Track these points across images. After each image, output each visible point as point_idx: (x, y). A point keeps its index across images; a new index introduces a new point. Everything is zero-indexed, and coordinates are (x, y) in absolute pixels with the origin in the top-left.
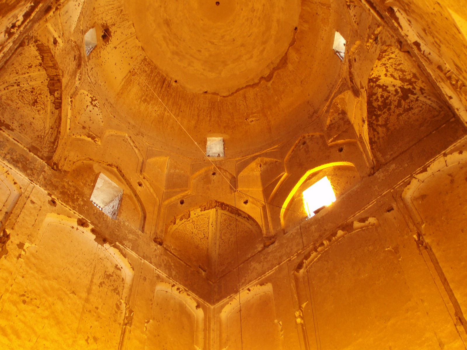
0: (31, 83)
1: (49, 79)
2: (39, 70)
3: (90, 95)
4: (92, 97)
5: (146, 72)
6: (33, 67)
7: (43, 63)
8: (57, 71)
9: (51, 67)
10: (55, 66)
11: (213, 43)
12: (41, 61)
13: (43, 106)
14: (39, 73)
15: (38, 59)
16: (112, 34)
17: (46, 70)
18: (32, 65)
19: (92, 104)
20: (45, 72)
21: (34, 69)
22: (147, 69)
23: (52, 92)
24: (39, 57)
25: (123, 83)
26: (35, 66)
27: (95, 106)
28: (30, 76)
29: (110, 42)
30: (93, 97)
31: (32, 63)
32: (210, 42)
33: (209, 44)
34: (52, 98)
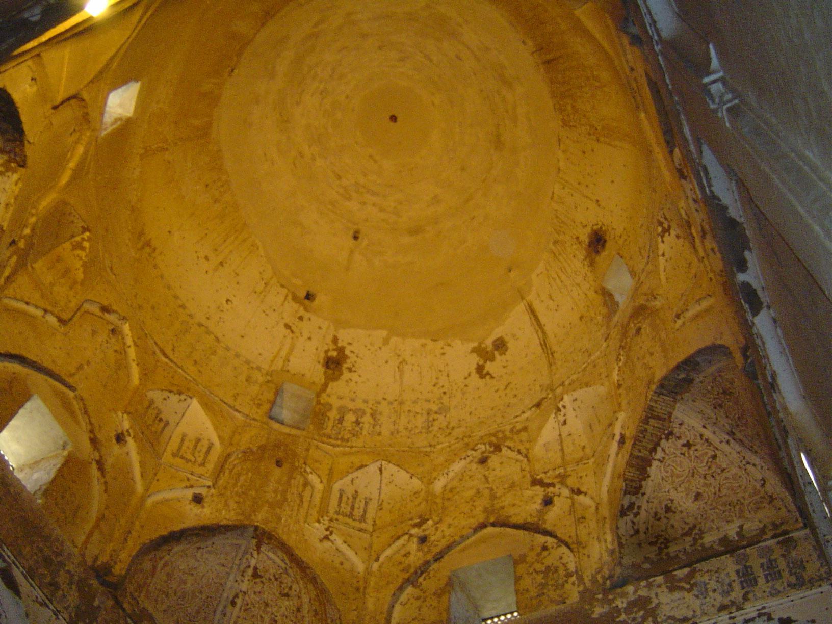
0: (713, 415)
1: (679, 397)
2: (681, 424)
3: (661, 246)
4: (659, 239)
5: (573, 107)
6: (683, 441)
7: (663, 436)
8: (653, 404)
9: (658, 418)
10: (650, 415)
11: (427, 57)
12: (663, 442)
13: (719, 379)
14: (686, 420)
15: (663, 450)
16: (588, 230)
17: (670, 415)
18: (684, 445)
19: (669, 227)
20: (675, 414)
21: (687, 433)
22: (569, 108)
23: (689, 381)
24: (659, 454)
25: (617, 143)
26: (679, 438)
27: (666, 219)
28: (704, 427)
29: (600, 224)
30: (658, 235)
31: (678, 453)
32: (431, 61)
33: (435, 59)
34: (693, 375)
